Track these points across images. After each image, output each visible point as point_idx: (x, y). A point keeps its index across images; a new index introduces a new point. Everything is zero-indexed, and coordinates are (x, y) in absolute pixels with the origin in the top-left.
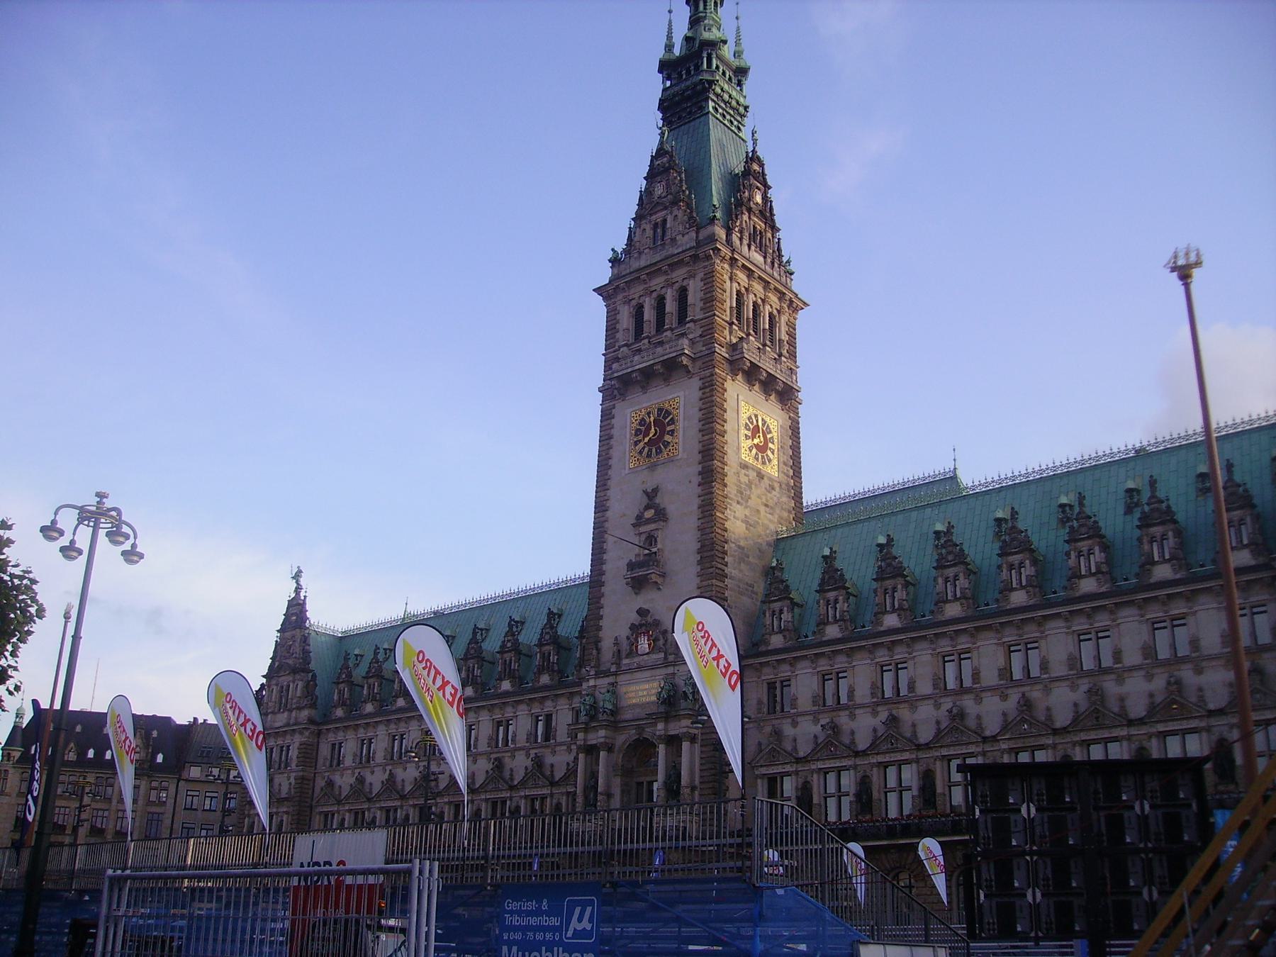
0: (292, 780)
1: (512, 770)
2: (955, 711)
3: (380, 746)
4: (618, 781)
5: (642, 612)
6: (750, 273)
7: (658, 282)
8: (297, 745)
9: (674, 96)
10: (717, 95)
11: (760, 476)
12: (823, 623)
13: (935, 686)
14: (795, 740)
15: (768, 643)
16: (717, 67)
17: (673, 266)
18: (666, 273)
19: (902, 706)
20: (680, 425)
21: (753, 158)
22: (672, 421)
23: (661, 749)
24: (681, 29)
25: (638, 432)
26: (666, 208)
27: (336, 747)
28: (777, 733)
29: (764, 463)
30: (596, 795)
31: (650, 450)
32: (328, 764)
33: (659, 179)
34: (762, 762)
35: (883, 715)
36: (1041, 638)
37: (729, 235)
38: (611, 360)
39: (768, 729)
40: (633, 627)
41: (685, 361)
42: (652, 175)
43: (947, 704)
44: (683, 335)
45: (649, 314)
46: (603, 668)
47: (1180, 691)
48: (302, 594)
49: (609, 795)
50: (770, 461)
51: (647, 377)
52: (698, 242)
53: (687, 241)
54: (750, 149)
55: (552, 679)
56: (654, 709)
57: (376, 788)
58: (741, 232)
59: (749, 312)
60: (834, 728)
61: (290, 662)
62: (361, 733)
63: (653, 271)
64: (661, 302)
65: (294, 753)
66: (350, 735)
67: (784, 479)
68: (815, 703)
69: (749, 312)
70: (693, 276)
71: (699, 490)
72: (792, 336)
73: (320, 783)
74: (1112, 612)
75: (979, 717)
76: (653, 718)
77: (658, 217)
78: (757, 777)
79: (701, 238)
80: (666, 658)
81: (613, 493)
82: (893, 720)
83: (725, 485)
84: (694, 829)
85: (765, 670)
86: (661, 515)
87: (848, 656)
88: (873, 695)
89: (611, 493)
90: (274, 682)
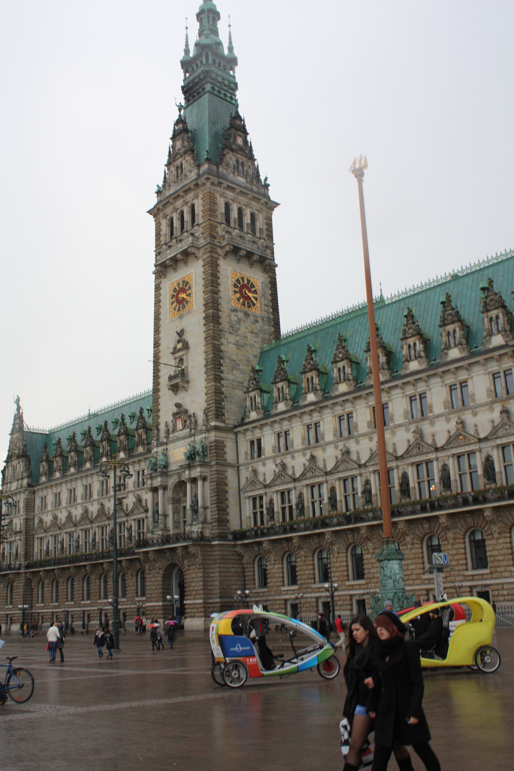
0: (22, 521)
1: (127, 505)
2: (344, 450)
3: (65, 496)
4: (170, 507)
5: (178, 405)
6: (233, 189)
7: (179, 203)
8: (22, 500)
9: (189, 83)
10: (214, 79)
11: (247, 315)
13: (335, 435)
14: (264, 474)
15: (249, 417)
16: (214, 62)
18: (183, 197)
19: (318, 449)
21: (238, 117)
22: (190, 288)
23: (188, 486)
25: (173, 296)
26: (181, 156)
27: (44, 499)
28: (255, 472)
29: (249, 307)
30: (158, 517)
31: (179, 307)
32: (40, 509)
33: (177, 138)
34: (248, 489)
35: (308, 457)
36: (389, 401)
39: (250, 469)
40: (174, 415)
41: (193, 250)
43: (341, 445)
45: (177, 224)
46: (161, 440)
47: (464, 427)
48: (21, 411)
49: (165, 516)
50: (254, 304)
53: (193, 176)
55: (144, 449)
56: (183, 463)
57: (64, 520)
59: (234, 214)
60: (284, 466)
61: (17, 452)
62: (55, 490)
63: (176, 197)
65: (22, 505)
66: (49, 491)
67: (265, 314)
68: (274, 451)
69: (234, 214)
70: (197, 197)
71: (204, 328)
72: (269, 225)
73: (37, 521)
74: (426, 381)
75: (358, 453)
77: (178, 163)
78: (245, 498)
79: (201, 172)
80: (191, 431)
82: (313, 458)
83: (220, 324)
84: (207, 533)
85: (249, 433)
86: (186, 346)
87: (289, 421)
88: (303, 443)
89: (160, 335)
90: (10, 464)
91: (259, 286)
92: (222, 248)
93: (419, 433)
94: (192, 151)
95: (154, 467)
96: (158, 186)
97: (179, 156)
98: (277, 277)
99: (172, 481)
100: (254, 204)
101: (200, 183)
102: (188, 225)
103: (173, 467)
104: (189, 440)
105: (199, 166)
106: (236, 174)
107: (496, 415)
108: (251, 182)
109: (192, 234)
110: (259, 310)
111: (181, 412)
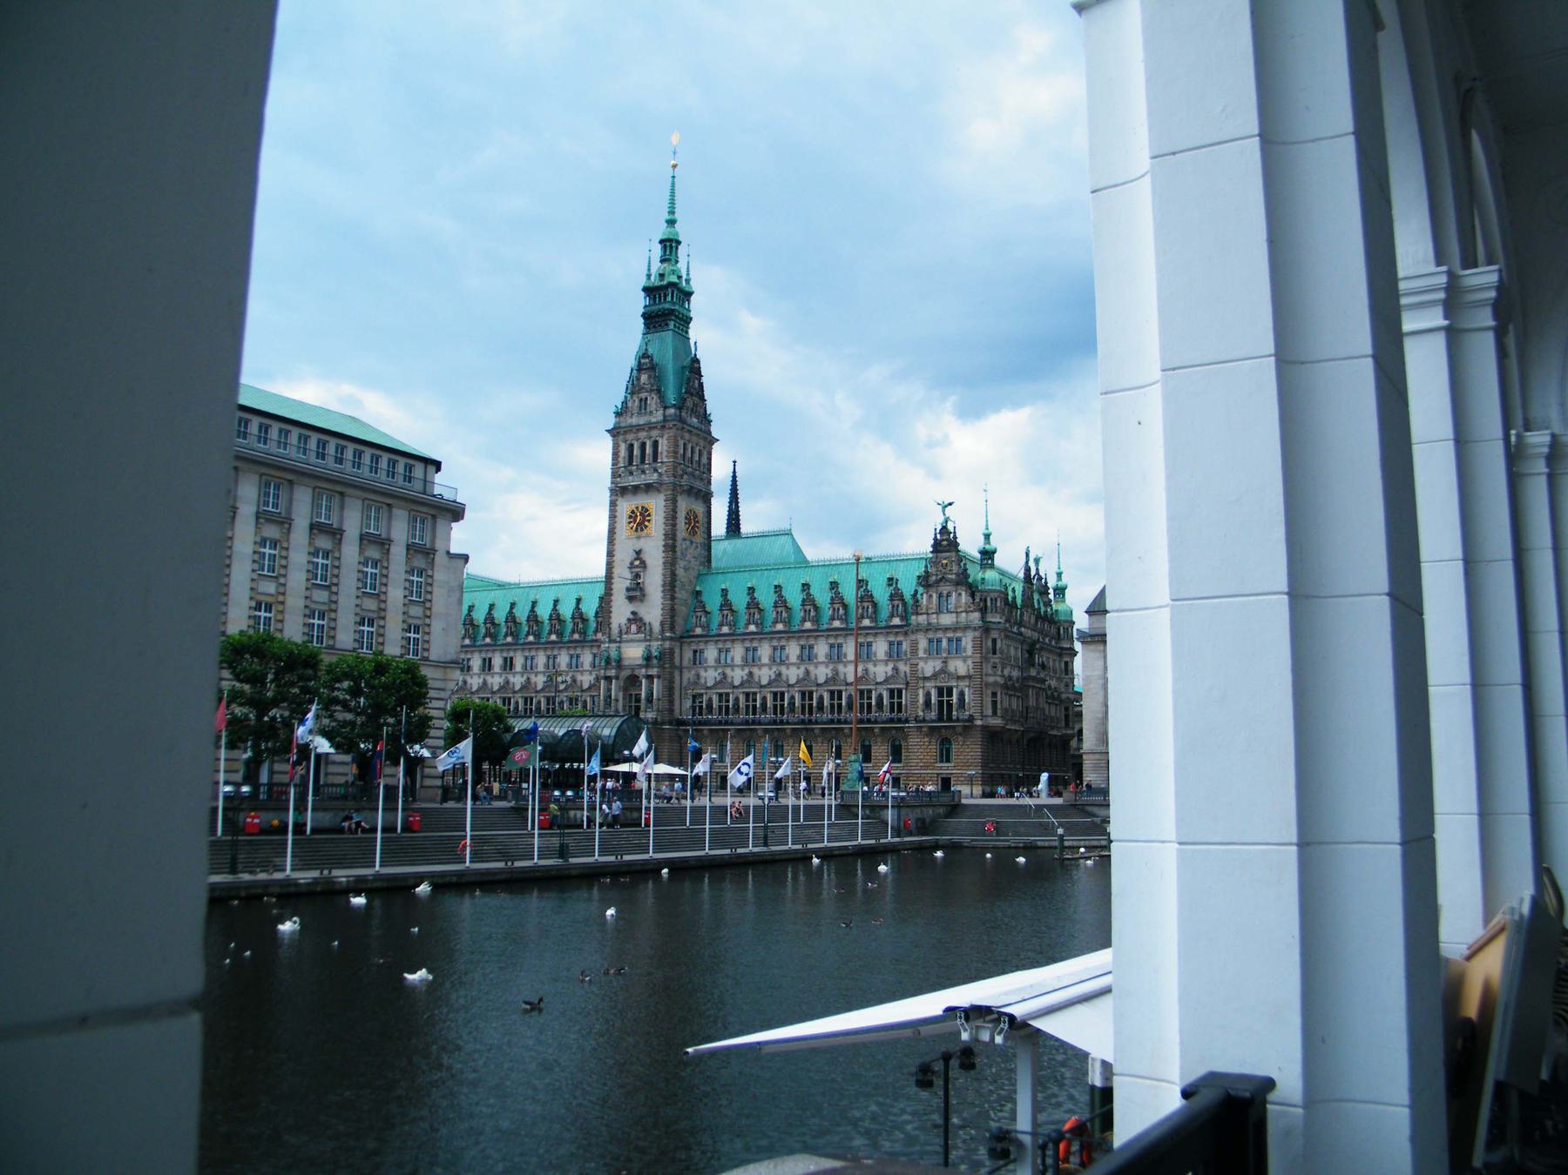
5: (634, 613)
7: (642, 435)
12: (721, 625)
20: (653, 517)
21: (696, 361)
24: (656, 266)
28: (698, 676)
35: (747, 671)
38: (615, 475)
42: (640, 368)
44: (656, 470)
45: (636, 452)
51: (636, 489)
63: (639, 428)
64: (643, 445)
76: (641, 666)
77: (643, 395)
81: (618, 547)
82: (751, 674)
86: (643, 565)
91: (701, 517)
93: (836, 673)
94: (659, 391)
95: (608, 661)
99: (625, 673)
100: (702, 443)
103: (626, 663)
104: (644, 644)
105: (665, 408)
107: (889, 668)
109: (656, 470)
110: (699, 539)
111: (635, 618)
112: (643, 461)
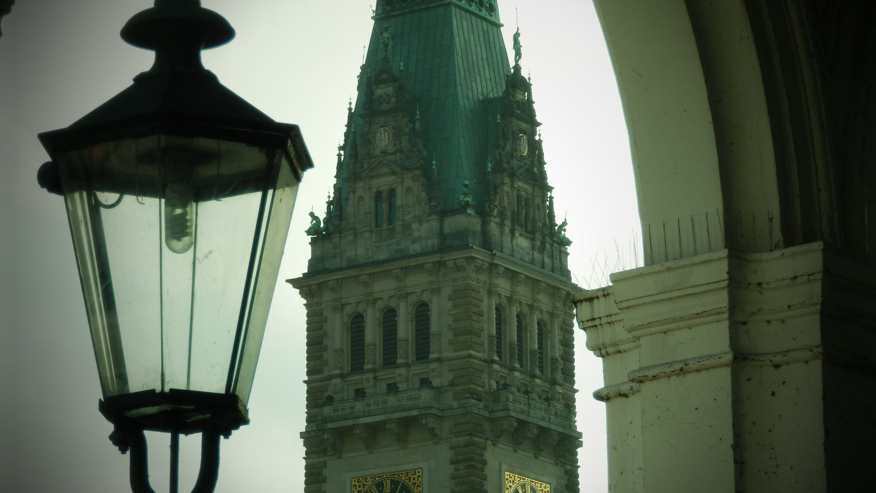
7: (384, 287)
17: (406, 270)
21: (518, 84)
26: (394, 173)
33: (381, 120)
37: (484, 224)
41: (431, 422)
44: (425, 382)
45: (372, 334)
51: (373, 433)
52: (442, 235)
54: (512, 64)
58: (502, 214)
64: (389, 317)
70: (437, 291)
79: (447, 230)
92: (492, 420)
96: (312, 214)
97: (385, 170)
98: (580, 471)
100: (544, 302)
101: (450, 264)
102: (406, 349)
106: (517, 234)
108: (542, 249)
109: (425, 382)
112: (390, 358)
